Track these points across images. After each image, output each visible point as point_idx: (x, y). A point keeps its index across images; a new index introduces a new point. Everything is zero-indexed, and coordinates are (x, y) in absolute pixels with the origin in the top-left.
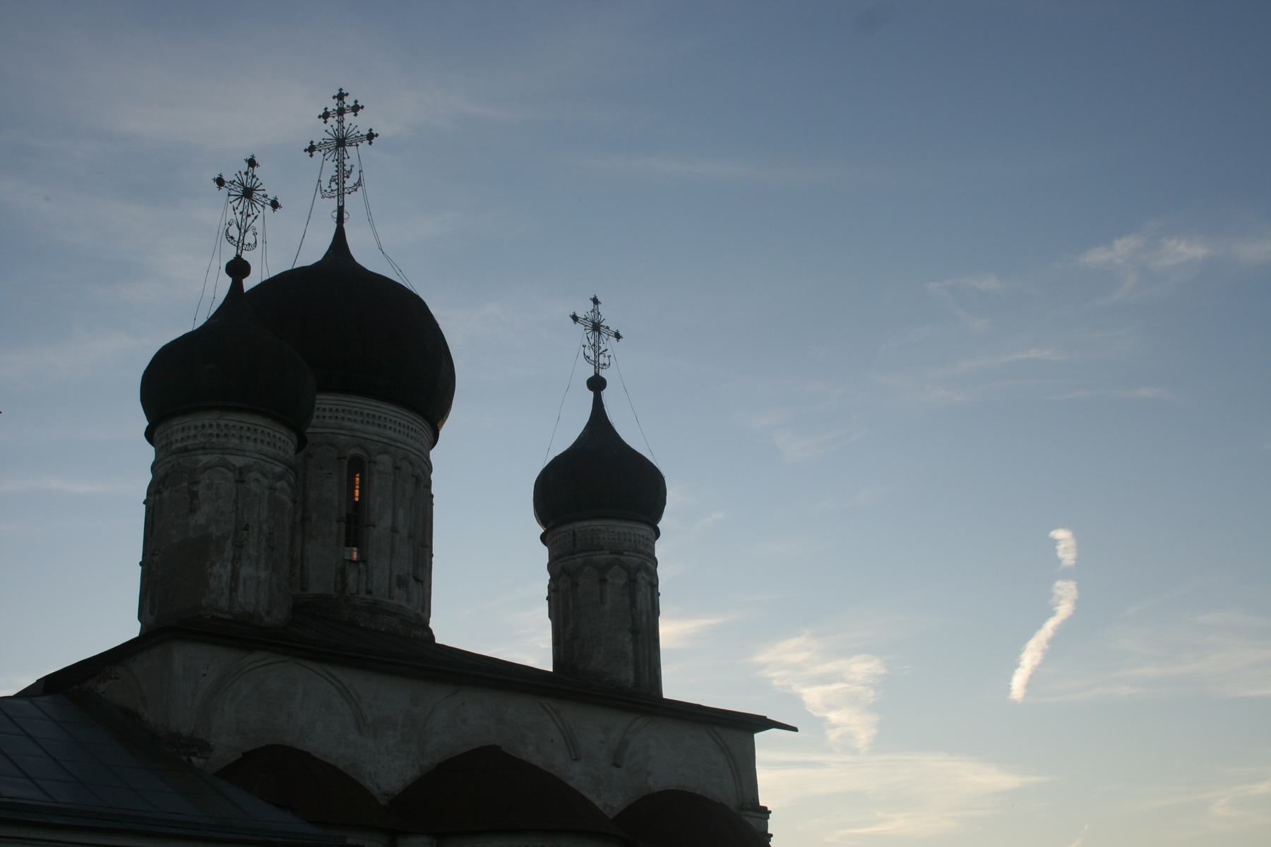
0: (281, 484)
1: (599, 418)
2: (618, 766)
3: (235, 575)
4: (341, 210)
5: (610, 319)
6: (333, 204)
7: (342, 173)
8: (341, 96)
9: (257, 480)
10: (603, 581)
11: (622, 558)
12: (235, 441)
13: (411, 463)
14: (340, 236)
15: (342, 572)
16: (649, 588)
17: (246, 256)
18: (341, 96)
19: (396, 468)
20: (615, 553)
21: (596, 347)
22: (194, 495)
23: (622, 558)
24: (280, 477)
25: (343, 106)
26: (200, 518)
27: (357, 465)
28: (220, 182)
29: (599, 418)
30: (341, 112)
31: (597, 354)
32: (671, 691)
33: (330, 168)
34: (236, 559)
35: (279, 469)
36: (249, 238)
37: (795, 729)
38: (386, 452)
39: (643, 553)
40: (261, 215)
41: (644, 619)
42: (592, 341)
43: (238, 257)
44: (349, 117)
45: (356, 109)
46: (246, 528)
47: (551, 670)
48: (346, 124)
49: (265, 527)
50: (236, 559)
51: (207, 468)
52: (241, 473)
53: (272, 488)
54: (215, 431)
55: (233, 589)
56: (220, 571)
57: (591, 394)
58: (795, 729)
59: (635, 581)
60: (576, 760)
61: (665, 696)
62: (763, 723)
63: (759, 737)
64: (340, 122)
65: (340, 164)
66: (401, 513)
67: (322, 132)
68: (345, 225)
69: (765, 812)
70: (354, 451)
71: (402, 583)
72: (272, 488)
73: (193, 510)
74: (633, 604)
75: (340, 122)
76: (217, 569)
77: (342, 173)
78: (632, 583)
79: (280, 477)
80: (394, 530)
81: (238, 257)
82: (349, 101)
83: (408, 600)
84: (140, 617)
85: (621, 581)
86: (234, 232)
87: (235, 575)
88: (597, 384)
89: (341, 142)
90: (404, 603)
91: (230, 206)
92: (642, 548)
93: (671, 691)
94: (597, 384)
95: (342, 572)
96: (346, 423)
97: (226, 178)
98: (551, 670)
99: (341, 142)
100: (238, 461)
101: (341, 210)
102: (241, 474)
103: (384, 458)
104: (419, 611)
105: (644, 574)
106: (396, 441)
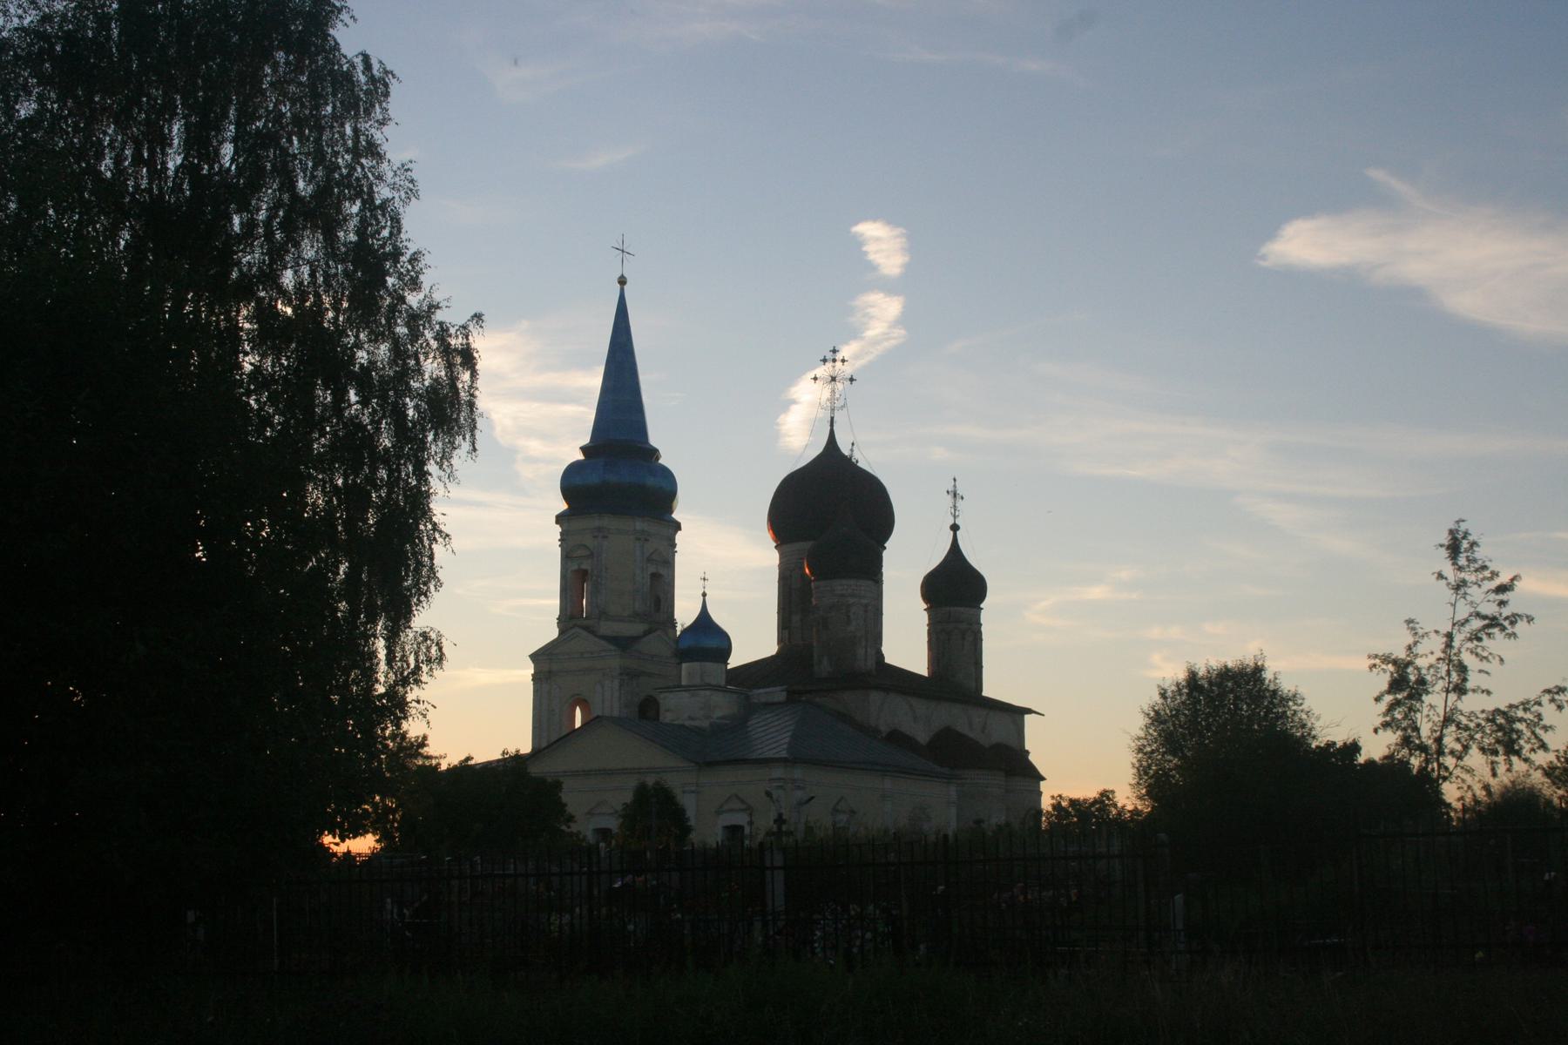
1: (955, 549)
3: (866, 651)
4: (832, 419)
10: (964, 639)
22: (849, 617)
29: (955, 547)
30: (834, 361)
32: (987, 692)
37: (1043, 715)
48: (837, 368)
57: (952, 533)
58: (1043, 715)
61: (985, 693)
62: (1029, 711)
63: (1027, 717)
68: (834, 428)
87: (866, 651)
88: (955, 528)
93: (987, 692)
94: (955, 528)
100: (865, 601)
101: (832, 419)
102: (866, 606)
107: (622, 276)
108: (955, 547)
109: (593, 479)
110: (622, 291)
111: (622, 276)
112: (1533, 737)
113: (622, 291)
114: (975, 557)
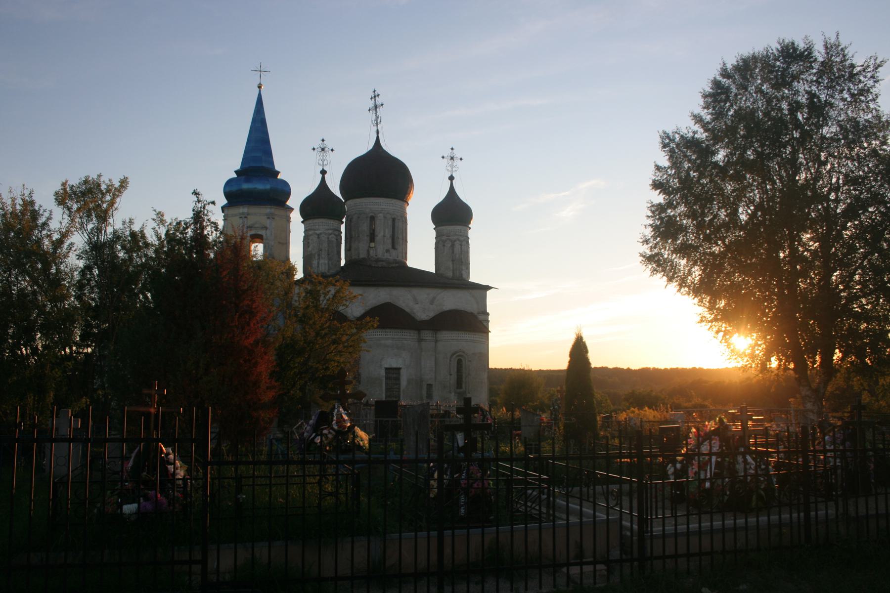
0: (333, 235)
1: (452, 191)
2: (432, 304)
3: (318, 263)
5: (457, 154)
6: (375, 128)
7: (377, 118)
8: (374, 92)
9: (323, 237)
10: (444, 246)
11: (450, 238)
12: (317, 227)
13: (390, 214)
14: (378, 138)
15: (368, 251)
16: (460, 246)
17: (325, 169)
18: (374, 92)
19: (384, 217)
20: (448, 236)
21: (452, 166)
22: (309, 243)
23: (450, 238)
24: (331, 234)
25: (375, 96)
26: (310, 249)
27: (373, 219)
28: (314, 149)
29: (452, 188)
30: (375, 97)
31: (452, 168)
33: (374, 117)
34: (319, 259)
35: (331, 232)
36: (325, 162)
38: (381, 213)
39: (457, 235)
40: (328, 155)
41: (457, 256)
42: (450, 164)
43: (323, 169)
44: (377, 98)
45: (378, 95)
46: (321, 250)
47: (434, 272)
49: (326, 249)
50: (319, 259)
51: (311, 235)
52: (318, 236)
53: (328, 238)
54: (312, 225)
55: (318, 267)
56: (315, 262)
57: (450, 181)
59: (454, 245)
60: (417, 303)
62: (489, 288)
64: (375, 100)
65: (376, 113)
66: (387, 231)
67: (371, 104)
69: (488, 314)
70: (371, 214)
71: (387, 251)
72: (328, 238)
73: (309, 247)
74: (453, 252)
75: (375, 100)
76: (314, 262)
77: (377, 118)
78: (453, 246)
79: (331, 234)
80: (384, 236)
81: (323, 169)
82: (376, 94)
83: (390, 256)
84: (303, 273)
85: (449, 245)
86: (321, 162)
87: (318, 263)
88: (451, 178)
89: (376, 107)
90: (389, 257)
91: (318, 155)
92: (458, 233)
94: (451, 178)
95: (368, 251)
96: (369, 206)
97: (315, 148)
98: (434, 272)
99: (376, 107)
100: (318, 232)
102: (319, 235)
103: (381, 214)
104: (396, 258)
105: (458, 242)
106: (385, 209)
107: (260, 84)
108: (452, 188)
109: (234, 188)
110: (260, 91)
111: (260, 84)
112: (376, 266)
113: (260, 91)
114: (463, 195)
